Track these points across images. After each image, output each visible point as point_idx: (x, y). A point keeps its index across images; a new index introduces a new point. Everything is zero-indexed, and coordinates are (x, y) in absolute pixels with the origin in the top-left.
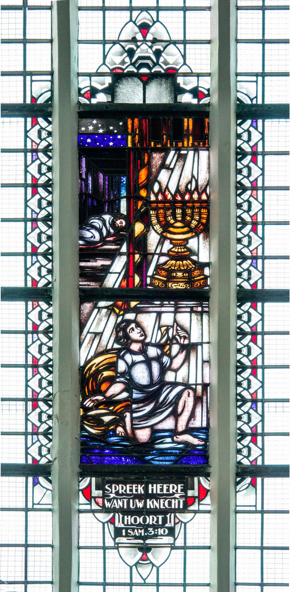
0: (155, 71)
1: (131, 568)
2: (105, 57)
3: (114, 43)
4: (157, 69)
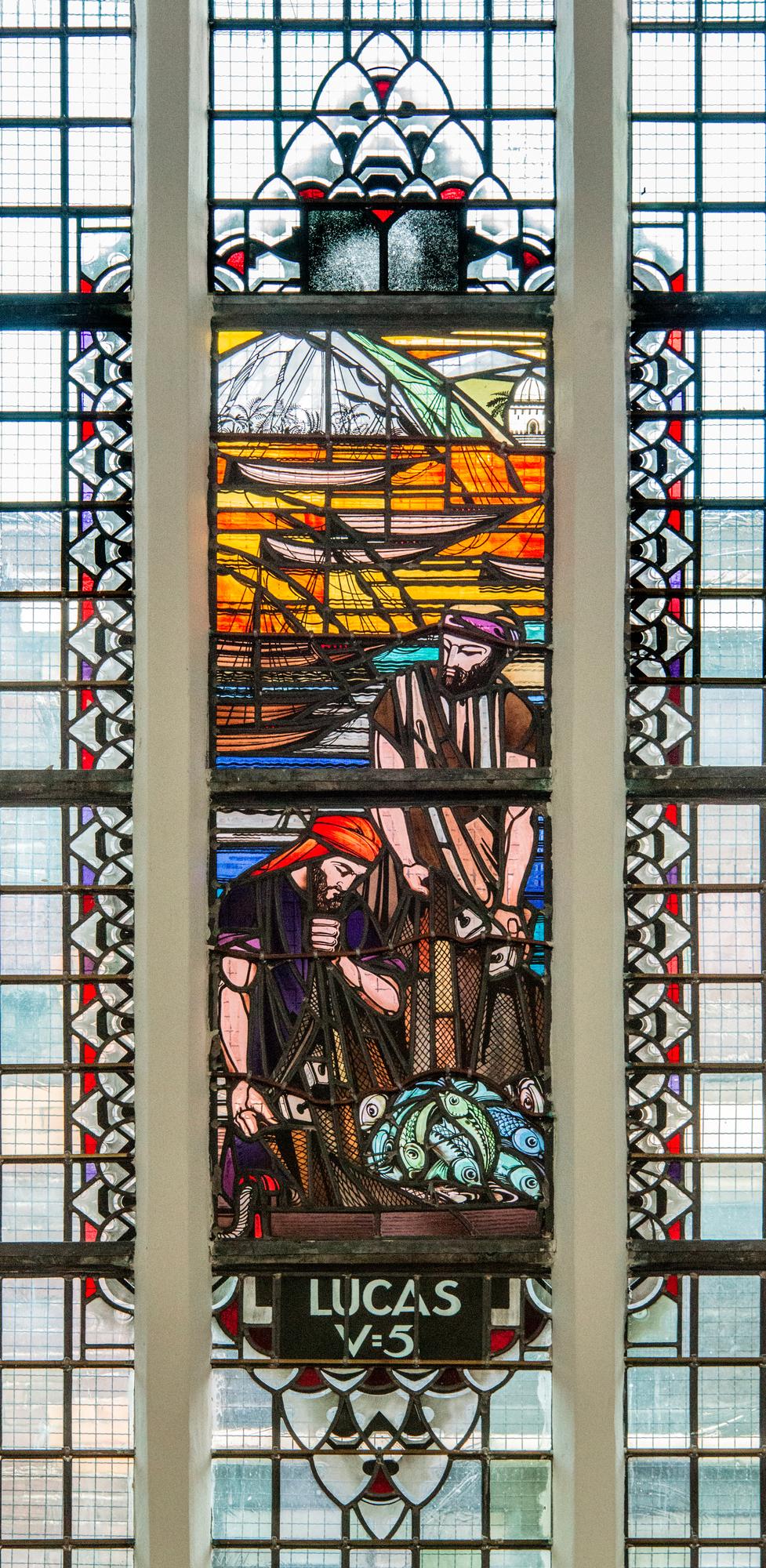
0: (411, 195)
1: (345, 1510)
2: (280, 153)
3: (309, 117)
4: (419, 187)
